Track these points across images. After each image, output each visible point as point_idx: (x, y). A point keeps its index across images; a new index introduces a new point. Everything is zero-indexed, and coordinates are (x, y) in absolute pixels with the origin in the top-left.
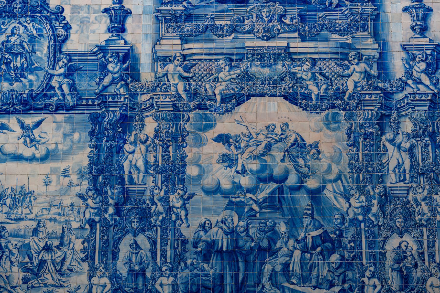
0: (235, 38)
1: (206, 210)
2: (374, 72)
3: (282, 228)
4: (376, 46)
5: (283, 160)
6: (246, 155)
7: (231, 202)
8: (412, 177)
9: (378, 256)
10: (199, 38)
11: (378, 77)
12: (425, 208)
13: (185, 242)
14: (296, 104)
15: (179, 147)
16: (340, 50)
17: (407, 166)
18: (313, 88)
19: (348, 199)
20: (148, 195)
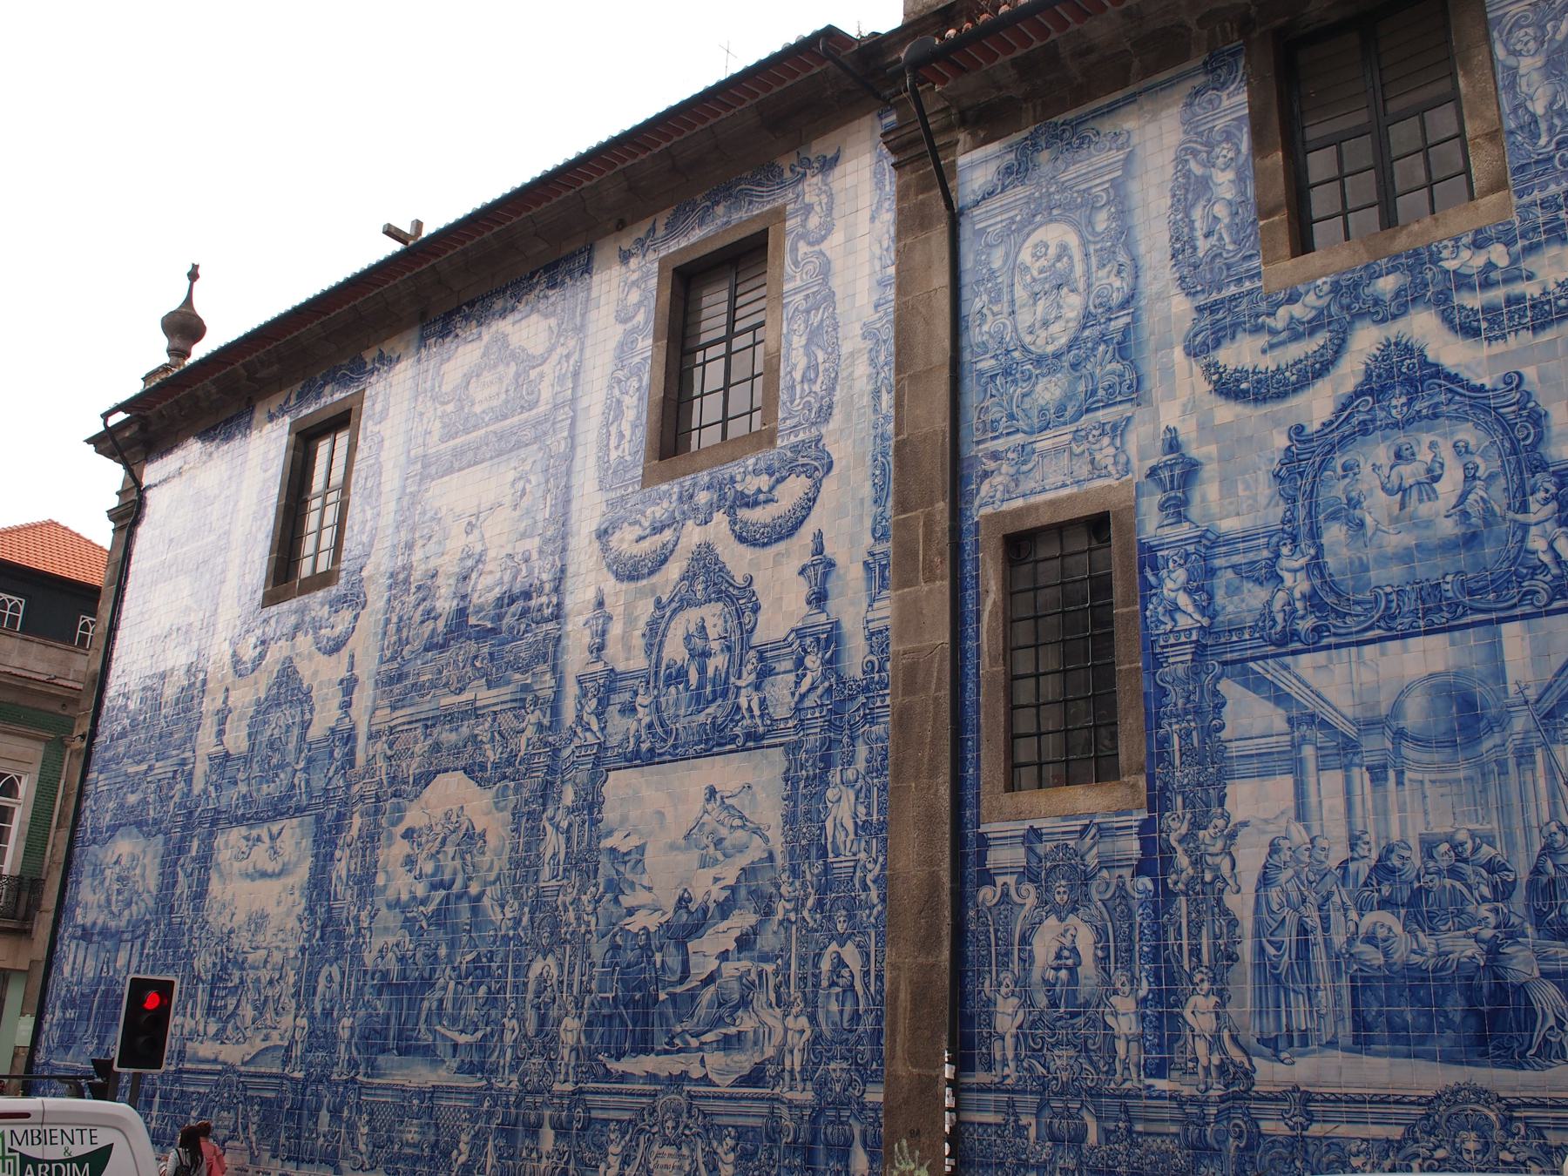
0: (434, 696)
1: (386, 929)
2: (546, 722)
3: (443, 951)
4: (553, 683)
5: (453, 859)
6: (424, 855)
7: (406, 917)
8: (565, 870)
9: (521, 987)
10: (405, 703)
11: (550, 728)
12: (571, 915)
13: (366, 972)
14: (472, 778)
15: (374, 848)
16: (519, 696)
17: (562, 856)
18: (490, 753)
19: (502, 907)
20: (345, 914)
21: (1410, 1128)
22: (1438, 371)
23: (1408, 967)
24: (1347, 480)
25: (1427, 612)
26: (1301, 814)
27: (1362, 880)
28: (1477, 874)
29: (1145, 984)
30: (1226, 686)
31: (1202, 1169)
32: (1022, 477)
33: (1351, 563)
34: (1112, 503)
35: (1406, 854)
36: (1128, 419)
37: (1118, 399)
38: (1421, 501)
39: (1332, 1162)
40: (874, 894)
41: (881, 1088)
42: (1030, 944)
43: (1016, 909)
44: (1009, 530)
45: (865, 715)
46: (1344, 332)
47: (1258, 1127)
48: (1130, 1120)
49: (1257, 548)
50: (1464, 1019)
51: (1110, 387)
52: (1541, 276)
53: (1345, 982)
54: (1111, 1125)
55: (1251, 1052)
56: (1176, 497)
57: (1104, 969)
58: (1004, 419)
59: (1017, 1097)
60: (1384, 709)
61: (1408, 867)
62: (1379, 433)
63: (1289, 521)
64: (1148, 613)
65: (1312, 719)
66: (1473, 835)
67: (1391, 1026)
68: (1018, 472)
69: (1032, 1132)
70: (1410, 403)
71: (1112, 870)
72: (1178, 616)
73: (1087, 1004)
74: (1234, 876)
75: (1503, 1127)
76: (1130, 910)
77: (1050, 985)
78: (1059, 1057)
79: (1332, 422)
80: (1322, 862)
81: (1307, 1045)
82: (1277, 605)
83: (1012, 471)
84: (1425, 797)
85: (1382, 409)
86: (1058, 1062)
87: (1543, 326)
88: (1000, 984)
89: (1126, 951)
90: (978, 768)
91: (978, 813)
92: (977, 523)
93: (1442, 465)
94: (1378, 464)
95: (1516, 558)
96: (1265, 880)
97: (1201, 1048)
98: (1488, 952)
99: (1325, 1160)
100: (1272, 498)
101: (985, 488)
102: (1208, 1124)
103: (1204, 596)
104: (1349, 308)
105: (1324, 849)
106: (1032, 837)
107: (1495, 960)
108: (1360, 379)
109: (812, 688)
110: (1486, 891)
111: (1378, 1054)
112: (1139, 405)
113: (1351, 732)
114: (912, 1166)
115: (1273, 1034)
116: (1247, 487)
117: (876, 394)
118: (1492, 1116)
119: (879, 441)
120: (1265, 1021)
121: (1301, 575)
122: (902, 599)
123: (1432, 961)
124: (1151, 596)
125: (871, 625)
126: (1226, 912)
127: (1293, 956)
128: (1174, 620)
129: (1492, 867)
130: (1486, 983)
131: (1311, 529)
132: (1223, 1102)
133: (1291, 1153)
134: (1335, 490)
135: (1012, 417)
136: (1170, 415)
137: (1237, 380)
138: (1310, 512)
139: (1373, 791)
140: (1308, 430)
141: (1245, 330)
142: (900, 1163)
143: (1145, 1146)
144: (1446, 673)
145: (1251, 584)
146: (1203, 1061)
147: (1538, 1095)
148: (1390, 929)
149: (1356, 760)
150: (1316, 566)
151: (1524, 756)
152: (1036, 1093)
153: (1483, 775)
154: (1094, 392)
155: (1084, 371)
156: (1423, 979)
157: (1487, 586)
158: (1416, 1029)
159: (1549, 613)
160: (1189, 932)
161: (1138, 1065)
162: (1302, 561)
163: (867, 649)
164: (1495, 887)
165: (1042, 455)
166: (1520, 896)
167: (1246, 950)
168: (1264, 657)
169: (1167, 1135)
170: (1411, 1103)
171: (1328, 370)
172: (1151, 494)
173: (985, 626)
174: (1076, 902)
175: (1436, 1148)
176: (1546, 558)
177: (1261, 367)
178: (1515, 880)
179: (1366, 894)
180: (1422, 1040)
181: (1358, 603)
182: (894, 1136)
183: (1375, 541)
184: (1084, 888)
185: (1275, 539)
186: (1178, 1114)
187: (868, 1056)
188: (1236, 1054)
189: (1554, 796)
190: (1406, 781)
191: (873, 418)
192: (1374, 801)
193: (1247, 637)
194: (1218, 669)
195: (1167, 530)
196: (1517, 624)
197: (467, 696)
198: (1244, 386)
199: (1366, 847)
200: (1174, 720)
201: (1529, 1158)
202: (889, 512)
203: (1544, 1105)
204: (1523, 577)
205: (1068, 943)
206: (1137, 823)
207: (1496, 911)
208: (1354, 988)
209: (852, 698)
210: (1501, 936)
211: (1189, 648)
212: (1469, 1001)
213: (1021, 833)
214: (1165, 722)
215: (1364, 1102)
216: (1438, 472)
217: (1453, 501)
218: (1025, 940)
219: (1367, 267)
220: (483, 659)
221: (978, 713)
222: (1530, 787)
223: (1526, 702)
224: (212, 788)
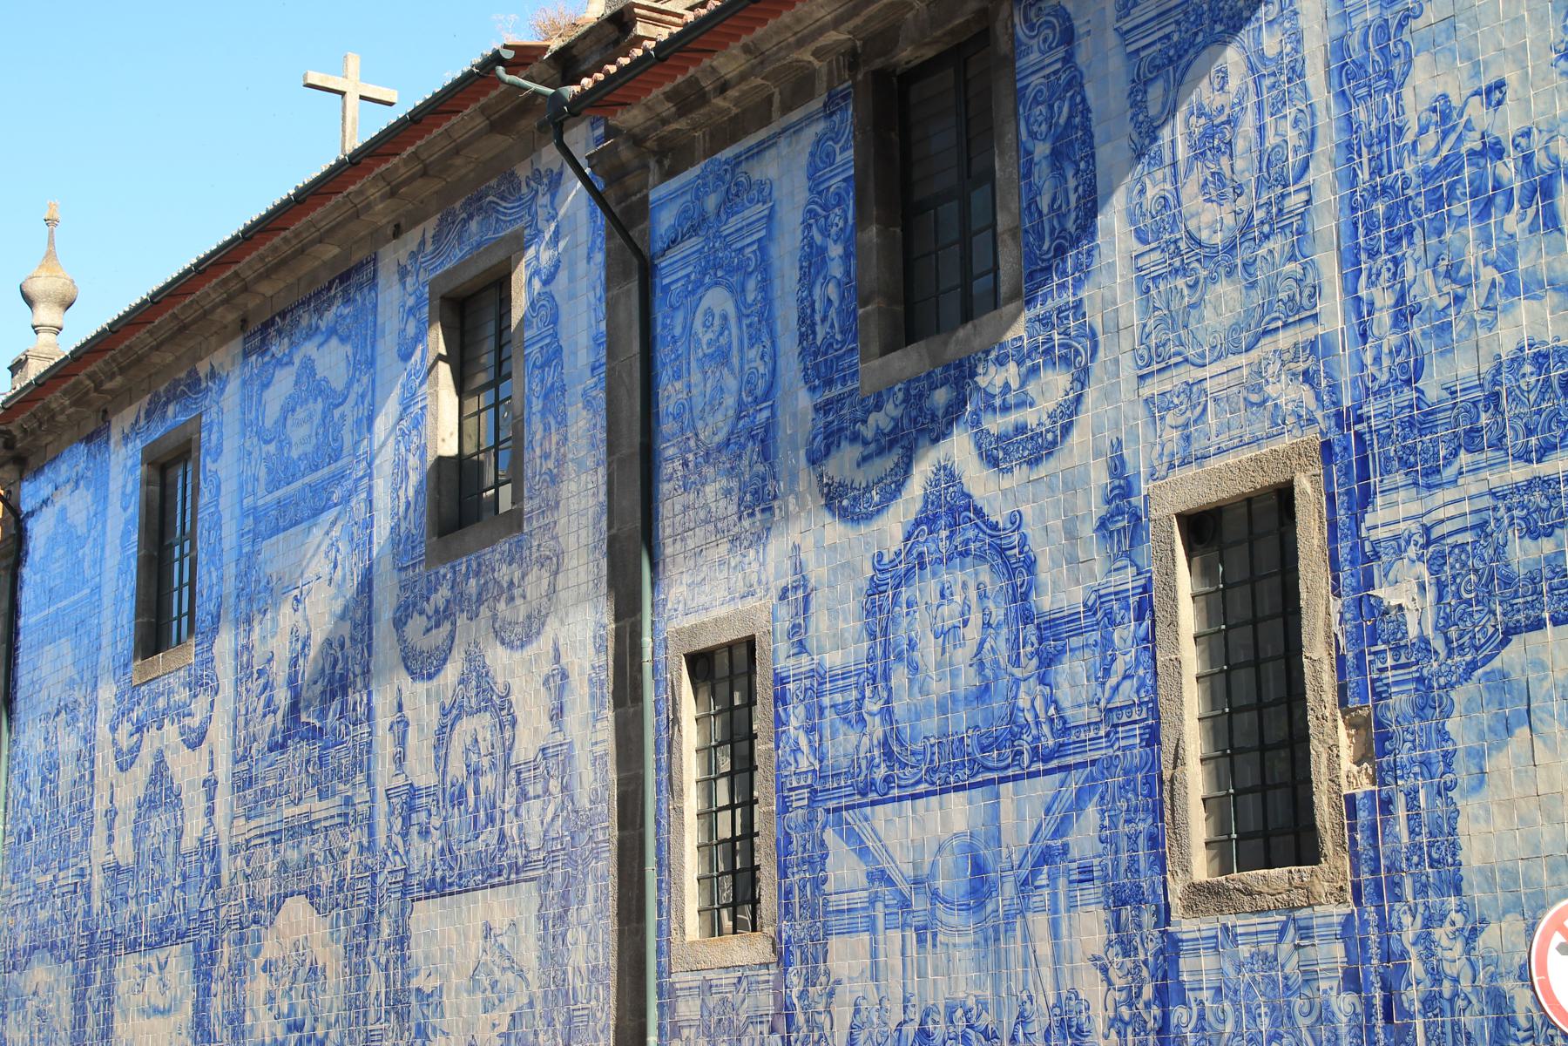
24: (909, 618)
30: (830, 836)
60: (926, 870)
66: (977, 1003)
108: (919, 505)
109: (556, 816)
113: (905, 888)
140: (886, 560)
150: (887, 713)
157: (991, 744)
159: (1031, 775)
168: (852, 807)
176: (1030, 717)
181: (913, 753)
183: (925, 688)
185: (862, 679)
189: (1025, 965)
197: (303, 808)
211: (805, 793)
220: (315, 764)
224: (107, 906)
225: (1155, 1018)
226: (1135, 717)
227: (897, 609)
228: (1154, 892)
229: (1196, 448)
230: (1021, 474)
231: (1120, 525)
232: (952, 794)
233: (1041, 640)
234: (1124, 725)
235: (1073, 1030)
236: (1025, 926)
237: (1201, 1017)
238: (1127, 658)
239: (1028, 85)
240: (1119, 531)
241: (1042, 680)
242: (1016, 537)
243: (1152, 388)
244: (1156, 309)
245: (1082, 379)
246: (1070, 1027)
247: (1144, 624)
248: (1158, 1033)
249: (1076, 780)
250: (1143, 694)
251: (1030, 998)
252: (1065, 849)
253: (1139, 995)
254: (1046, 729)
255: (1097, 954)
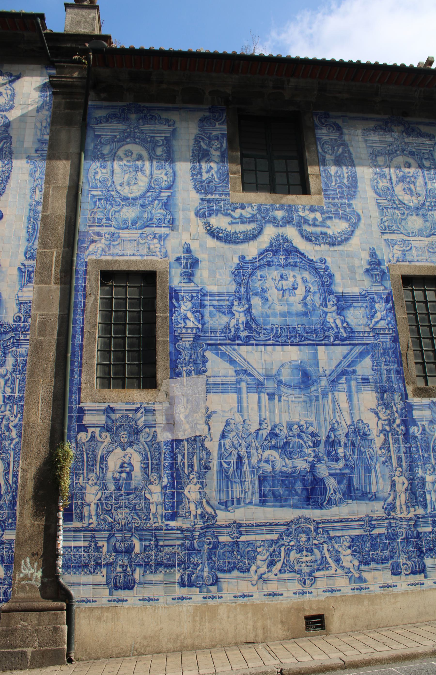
21: (281, 535)
22: (296, 250)
23: (281, 472)
24: (262, 282)
25: (291, 337)
26: (240, 410)
27: (264, 437)
28: (307, 437)
29: (166, 480)
30: (208, 354)
31: (192, 559)
32: (112, 247)
33: (262, 314)
34: (159, 267)
35: (281, 428)
36: (167, 235)
37: (163, 225)
38: (290, 296)
39: (249, 551)
40: (14, 434)
41: (14, 532)
42: (106, 461)
43: (99, 444)
44: (104, 268)
45: (13, 343)
46: (262, 226)
47: (218, 539)
48: (157, 540)
49: (224, 300)
50: (302, 491)
51: (159, 219)
52: (332, 227)
53: (256, 479)
54: (147, 543)
55: (215, 508)
56: (188, 272)
57: (145, 473)
58: (105, 219)
59: (96, 533)
60: (274, 372)
61: (282, 433)
62: (273, 267)
63: (238, 292)
64: (173, 318)
65: (245, 372)
66: (306, 423)
67: (274, 495)
68: (110, 244)
69: (105, 549)
70: (286, 259)
71: (151, 428)
72: (187, 321)
73: (136, 489)
74: (210, 434)
75: (315, 531)
76: (159, 446)
77: (117, 480)
78: (121, 513)
79: (256, 258)
80: (248, 430)
81: (240, 504)
82: (232, 325)
83: (107, 243)
84: (289, 407)
85: (276, 258)
86: (120, 516)
87: (333, 245)
88: (89, 480)
89: (157, 465)
90: (80, 375)
91: (79, 398)
92: (86, 262)
93: (298, 284)
94: (274, 278)
95: (323, 323)
96: (223, 436)
97: (192, 507)
98: (311, 466)
99: (247, 550)
100: (231, 281)
101: (92, 247)
102: (195, 539)
103: (200, 315)
104: (264, 218)
105: (248, 425)
106: (109, 411)
107: (313, 469)
108: (267, 245)
110: (311, 444)
111: (269, 506)
112: (173, 230)
113: (261, 379)
114: (32, 571)
115: (225, 500)
116: (220, 275)
117: (33, 190)
118: (312, 527)
119: (32, 212)
120: (222, 495)
121: (242, 314)
122: (40, 289)
123: (290, 470)
124: (175, 311)
125: (20, 299)
126: (205, 449)
127: (235, 468)
128: (185, 322)
129: (312, 435)
130: (310, 478)
131: (247, 297)
132: (202, 529)
133: (232, 549)
134: (257, 285)
135: (108, 219)
136: (186, 238)
137: (218, 232)
138: (246, 290)
139: (269, 403)
140: (247, 259)
141: (222, 214)
142: (24, 570)
143: (165, 551)
144: (297, 361)
145: (221, 314)
146: (194, 513)
147: (327, 518)
148: (275, 457)
149: (263, 390)
150: (248, 312)
151: (325, 395)
152: (107, 530)
153: (311, 400)
154: (151, 219)
155: (147, 209)
156: (287, 477)
158: (284, 496)
159: (334, 345)
160: (188, 457)
161: (162, 516)
162: (243, 309)
163: (17, 310)
164: (314, 442)
165: (124, 239)
166: (322, 446)
167: (214, 465)
168: (225, 345)
169: (175, 545)
170: (281, 525)
171: (255, 238)
172: (177, 268)
173: (89, 310)
174: (132, 442)
175: (291, 541)
176: (333, 325)
177: (229, 230)
178: (321, 440)
179: (266, 443)
180: (286, 500)
181: (265, 329)
182: (22, 556)
183: (272, 307)
184: (136, 436)
185: (232, 298)
186: (181, 536)
187: (6, 516)
188: (209, 509)
189: (334, 410)
190: (282, 400)
191: (30, 201)
192: (269, 407)
193: (218, 335)
194: (205, 347)
195: (183, 285)
196: (323, 347)
198: (221, 235)
199: (266, 425)
200: (183, 365)
201: (324, 542)
202: (36, 246)
203: (329, 522)
204: (326, 330)
205: (127, 460)
206: (164, 408)
207: (314, 451)
208: (260, 481)
209: (6, 333)
210: (315, 460)
211: (192, 336)
212: (304, 485)
213: (103, 408)
214: (179, 366)
215: (263, 526)
216: (296, 286)
217: (302, 299)
218: (103, 459)
219: (272, 205)
221: (82, 350)
222: (326, 407)
223: (326, 375)
225: (402, 430)
226: (386, 332)
227: (254, 277)
228: (400, 389)
229: (408, 257)
230: (324, 248)
231: (376, 273)
232: (290, 346)
233: (338, 301)
234: (381, 334)
235: (361, 434)
236: (334, 396)
237: (424, 430)
238: (382, 313)
239: (321, 138)
240: (375, 275)
241: (339, 314)
242: (323, 266)
243: (386, 237)
244: (386, 215)
245: (354, 226)
246: (359, 433)
247: (389, 305)
248: (404, 435)
249: (358, 350)
250: (390, 325)
251: (337, 422)
252: (354, 372)
253: (394, 422)
254: (342, 330)
255: (372, 407)
